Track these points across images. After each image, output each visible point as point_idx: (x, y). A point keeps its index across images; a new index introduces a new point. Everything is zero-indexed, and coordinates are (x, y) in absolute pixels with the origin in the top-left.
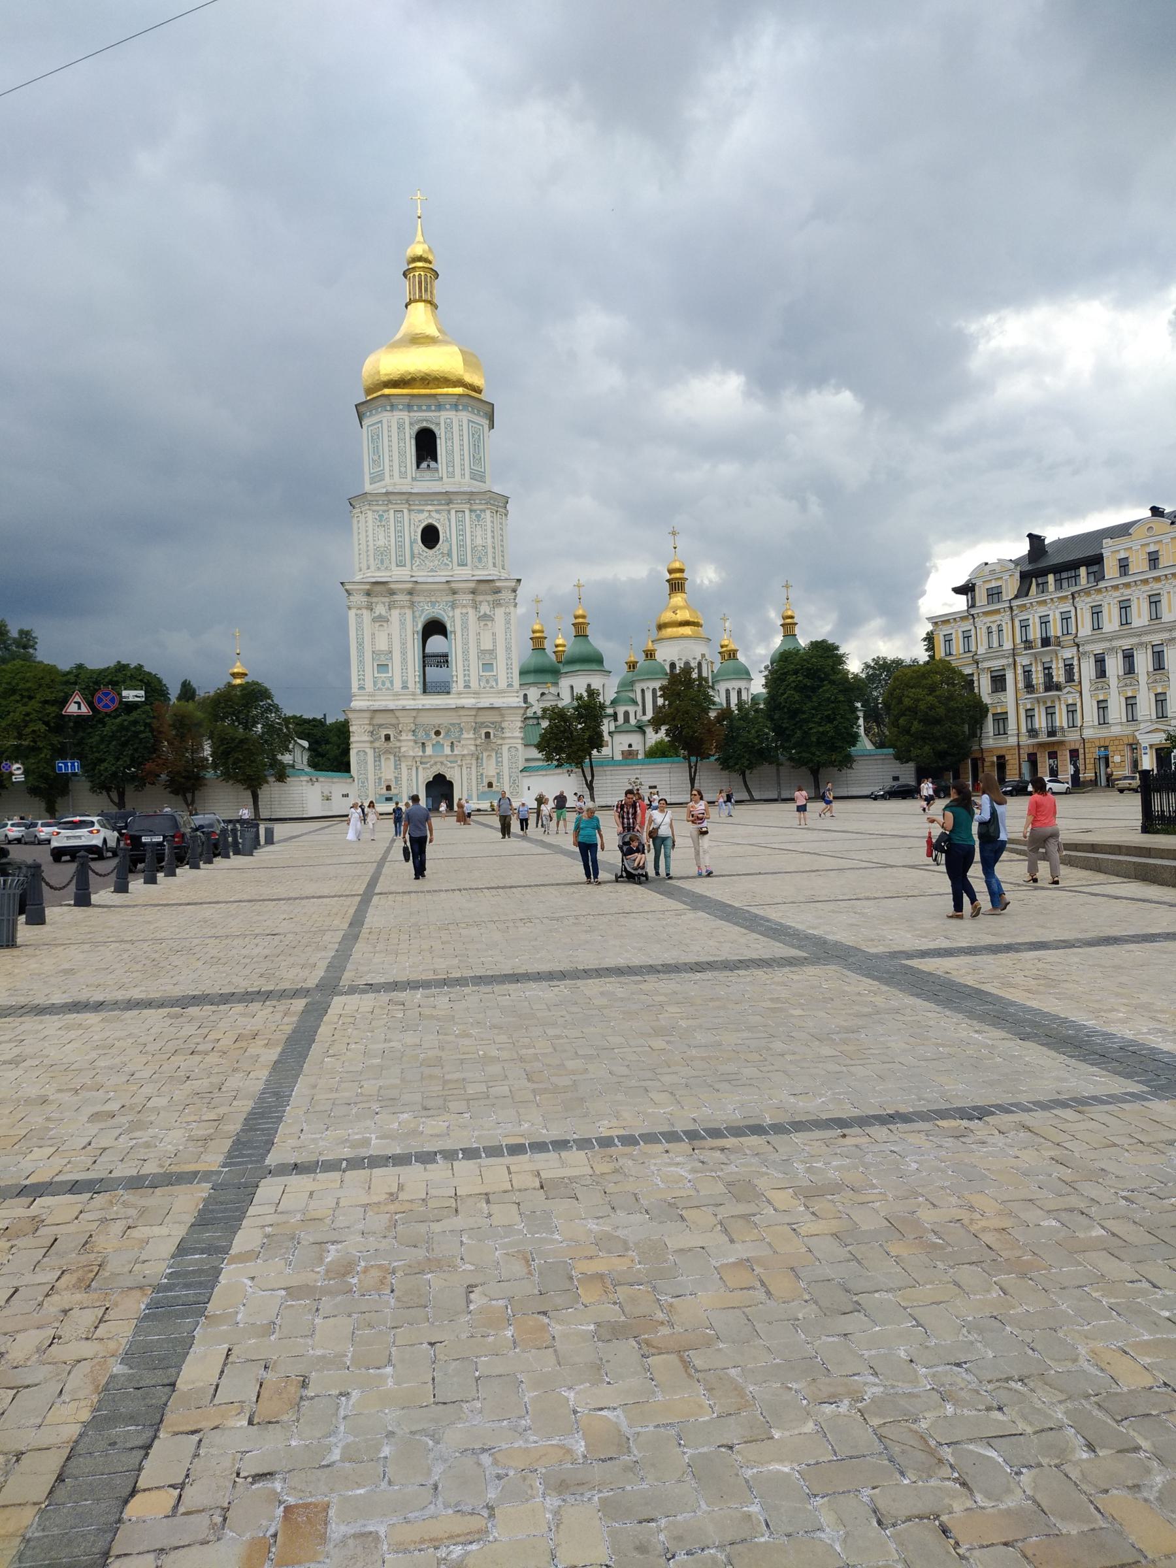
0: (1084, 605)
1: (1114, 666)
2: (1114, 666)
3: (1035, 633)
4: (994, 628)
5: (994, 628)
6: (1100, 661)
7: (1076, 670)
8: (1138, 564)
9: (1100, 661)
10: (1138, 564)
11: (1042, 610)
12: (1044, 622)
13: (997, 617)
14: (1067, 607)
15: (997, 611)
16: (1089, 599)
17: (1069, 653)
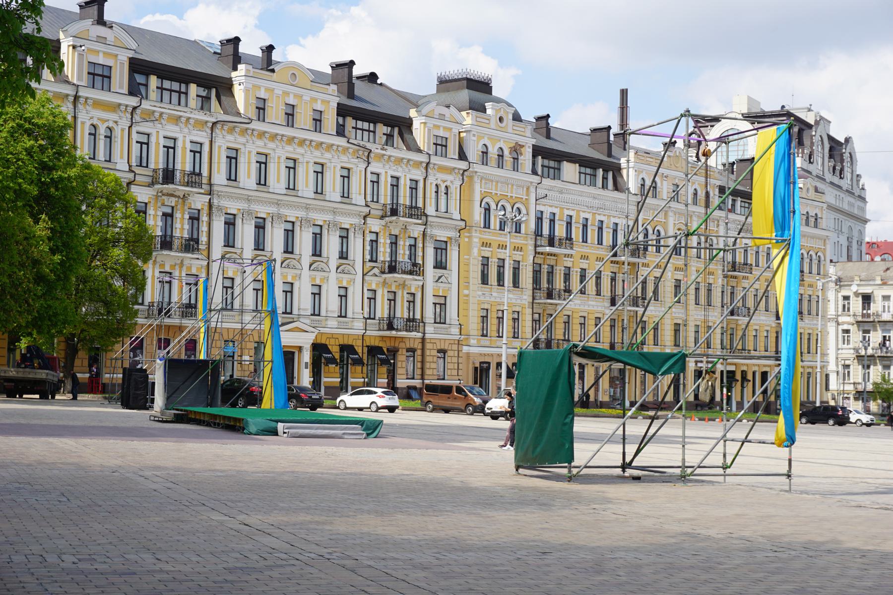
0: (224, 141)
1: (246, 233)
2: (246, 233)
3: (157, 160)
4: (102, 131)
5: (102, 131)
6: (230, 224)
7: (204, 228)
8: (275, 112)
9: (230, 224)
10: (275, 112)
11: (172, 130)
12: (170, 149)
13: (113, 116)
14: (202, 137)
15: (115, 107)
16: (230, 137)
17: (199, 201)
